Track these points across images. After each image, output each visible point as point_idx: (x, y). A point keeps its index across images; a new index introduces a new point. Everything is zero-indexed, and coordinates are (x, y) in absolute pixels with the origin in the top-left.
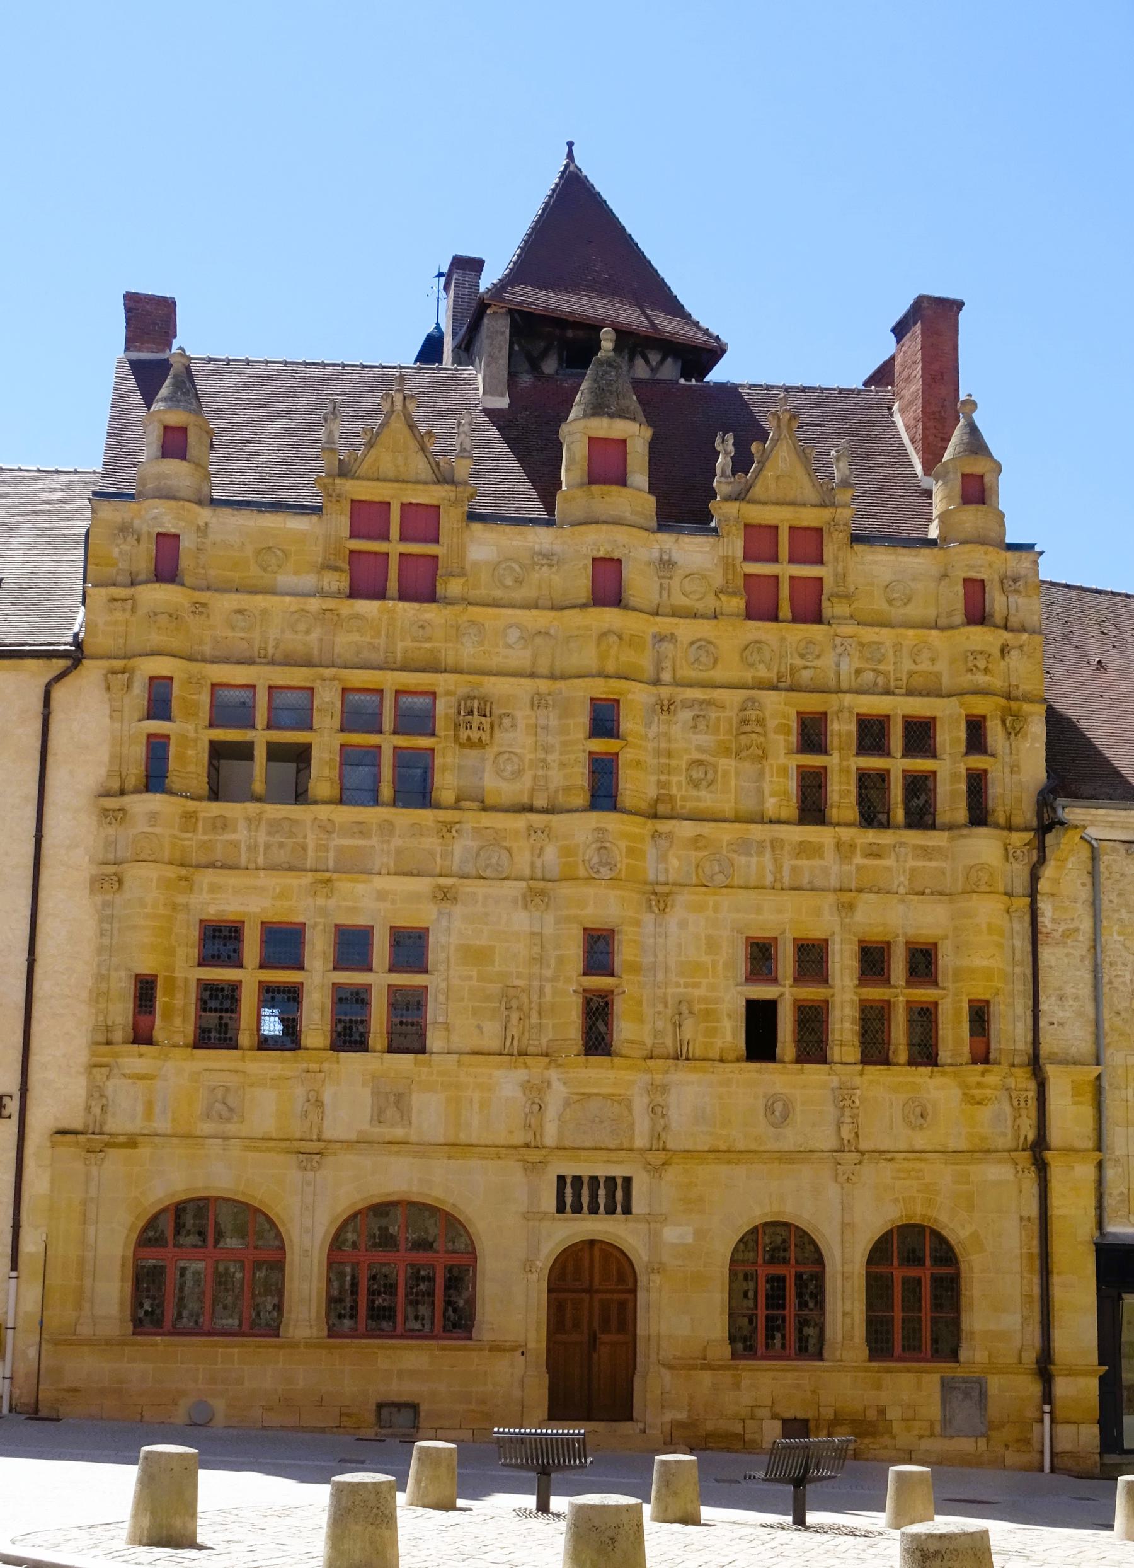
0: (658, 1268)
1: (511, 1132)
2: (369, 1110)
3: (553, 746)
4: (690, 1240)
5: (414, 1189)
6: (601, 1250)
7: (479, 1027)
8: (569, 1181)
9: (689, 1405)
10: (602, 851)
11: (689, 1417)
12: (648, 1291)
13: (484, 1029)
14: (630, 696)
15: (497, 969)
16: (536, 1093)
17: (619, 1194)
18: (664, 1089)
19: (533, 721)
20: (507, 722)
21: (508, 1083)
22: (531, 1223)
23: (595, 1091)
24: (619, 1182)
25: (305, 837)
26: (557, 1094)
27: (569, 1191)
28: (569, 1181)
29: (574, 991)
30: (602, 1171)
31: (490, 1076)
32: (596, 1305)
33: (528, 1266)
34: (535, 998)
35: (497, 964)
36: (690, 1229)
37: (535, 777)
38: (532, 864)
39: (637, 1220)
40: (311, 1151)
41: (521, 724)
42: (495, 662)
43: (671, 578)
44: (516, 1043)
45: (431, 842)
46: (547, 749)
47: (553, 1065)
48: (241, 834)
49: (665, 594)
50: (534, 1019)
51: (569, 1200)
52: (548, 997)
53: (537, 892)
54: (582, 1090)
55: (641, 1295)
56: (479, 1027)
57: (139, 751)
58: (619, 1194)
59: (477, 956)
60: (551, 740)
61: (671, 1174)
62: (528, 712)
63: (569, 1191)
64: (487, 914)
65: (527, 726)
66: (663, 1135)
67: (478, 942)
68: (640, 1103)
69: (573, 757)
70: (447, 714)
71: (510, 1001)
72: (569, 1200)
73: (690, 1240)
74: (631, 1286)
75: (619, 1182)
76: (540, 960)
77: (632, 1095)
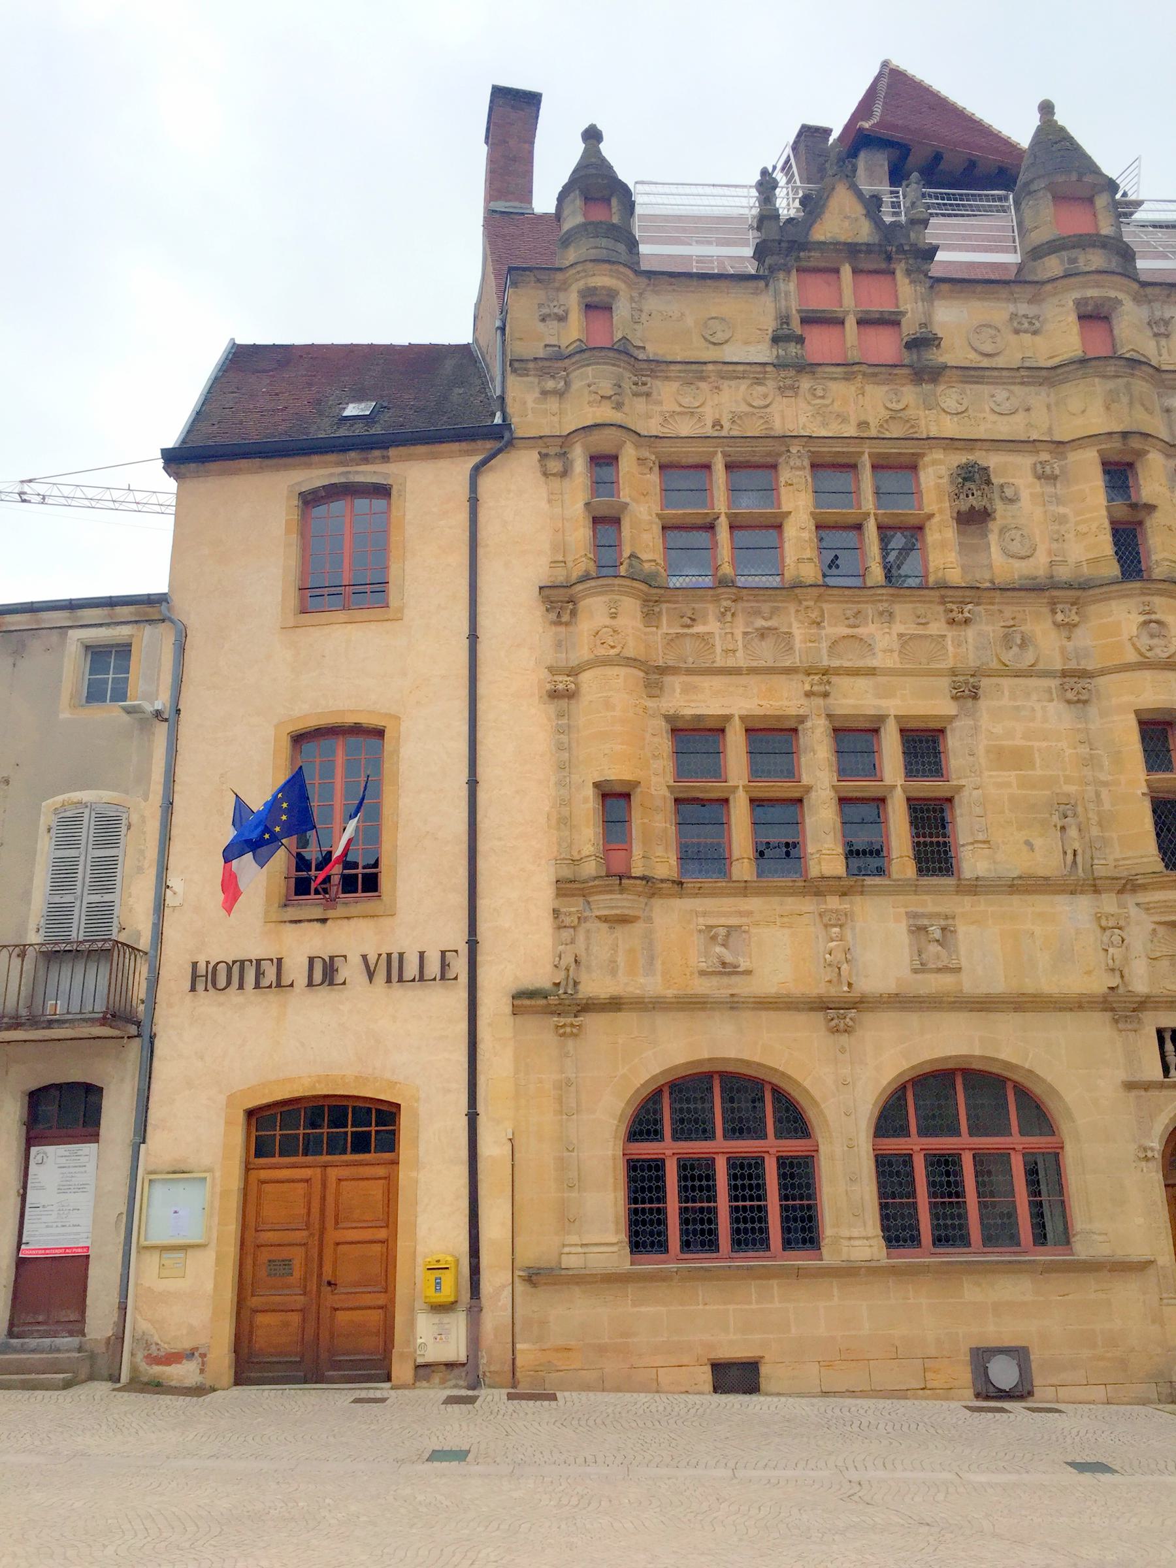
1: (1089, 973)
2: (907, 950)
3: (1065, 516)
5: (977, 1052)
7: (1028, 843)
8: (1168, 1036)
10: (1153, 625)
13: (1036, 848)
14: (1151, 456)
15: (1039, 772)
19: (1038, 489)
20: (1009, 492)
21: (1076, 914)
22: (1134, 1093)
25: (790, 626)
29: (1143, 794)
34: (1091, 806)
35: (1038, 765)
37: (1050, 552)
38: (1063, 650)
40: (840, 1010)
41: (1025, 495)
42: (980, 432)
43: (1167, 336)
44: (1079, 859)
45: (937, 627)
46: (1061, 519)
48: (710, 626)
49: (1164, 351)
50: (1095, 831)
52: (1107, 806)
53: (1076, 683)
56: (1028, 843)
57: (580, 534)
59: (1011, 758)
60: (1062, 510)
62: (1031, 479)
64: (1017, 708)
65: (1031, 494)
67: (1010, 743)
69: (1094, 526)
70: (938, 486)
71: (1065, 811)
76: (1090, 762)
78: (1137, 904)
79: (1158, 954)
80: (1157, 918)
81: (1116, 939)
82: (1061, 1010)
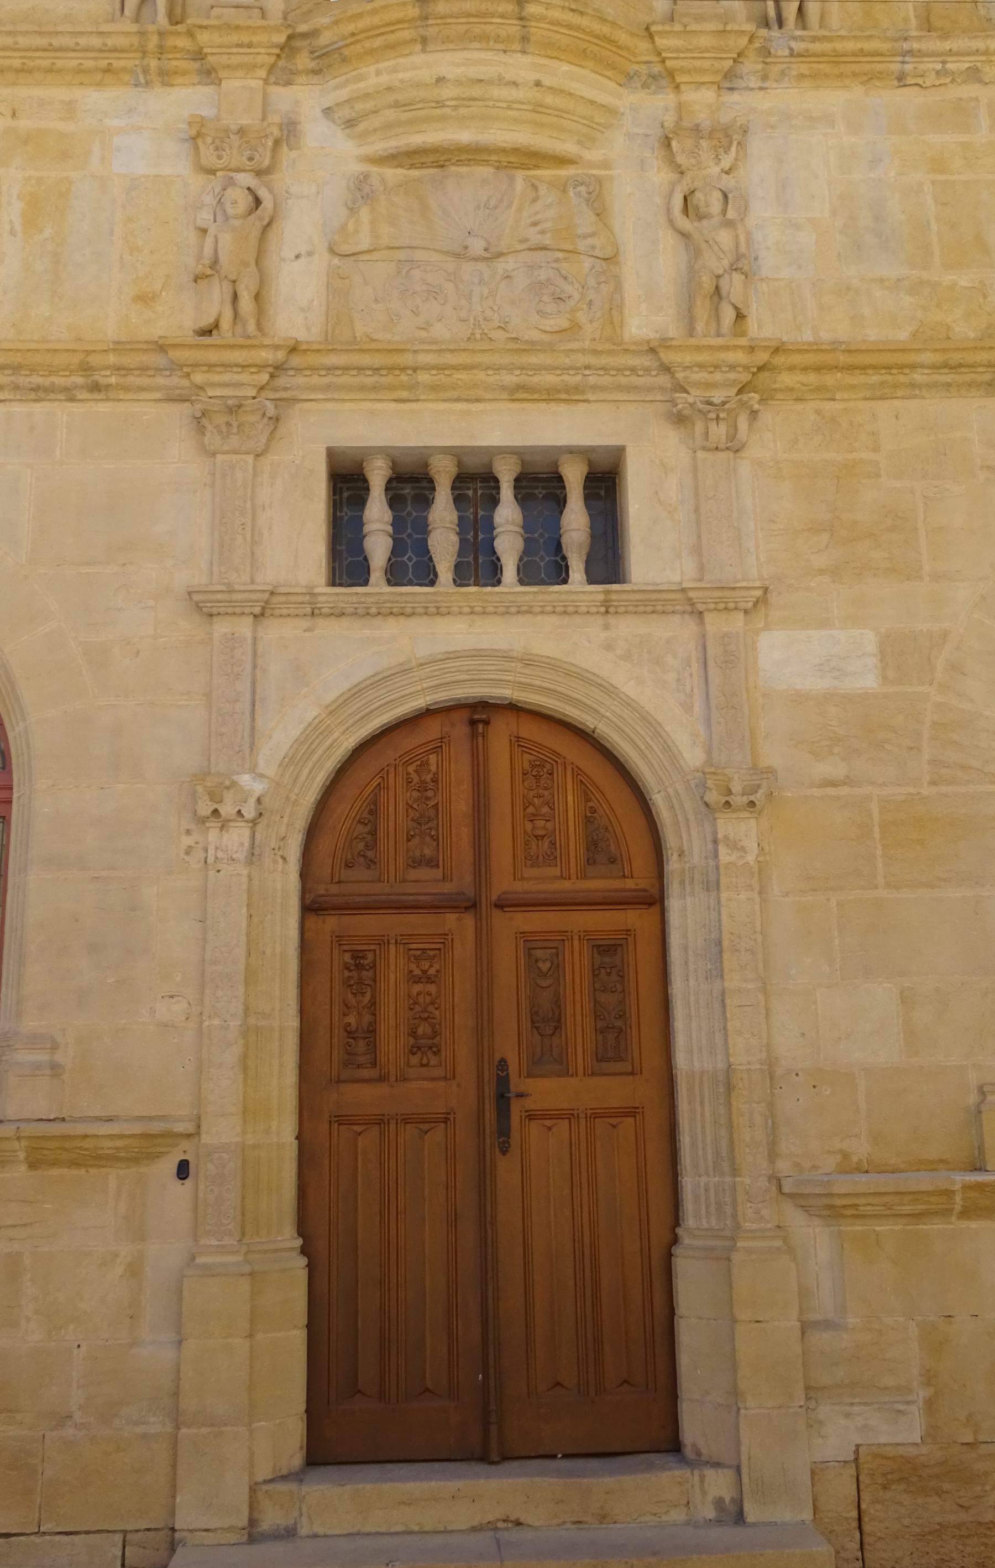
0: (754, 796)
1: (145, 299)
4: (867, 680)
6: (517, 741)
8: (378, 477)
9: (929, 1378)
11: (932, 1434)
12: (713, 886)
16: (246, 165)
17: (576, 521)
18: (728, 137)
22: (222, 627)
23: (465, 136)
24: (574, 476)
26: (325, 160)
27: (377, 513)
28: (378, 477)
30: (503, 429)
31: (70, 110)
32: (507, 958)
33: (208, 801)
36: (869, 640)
39: (655, 604)
47: (303, 61)
51: (378, 547)
54: (417, 139)
55: (684, 911)
58: (576, 521)
61: (775, 436)
63: (377, 513)
66: (734, 286)
68: (637, 191)
72: (378, 547)
73: (867, 680)
74: (639, 881)
75: (574, 476)
77: (605, 164)
78: (327, 112)
79: (364, 242)
80: (381, 146)
81: (238, 200)
82: (40, 393)
